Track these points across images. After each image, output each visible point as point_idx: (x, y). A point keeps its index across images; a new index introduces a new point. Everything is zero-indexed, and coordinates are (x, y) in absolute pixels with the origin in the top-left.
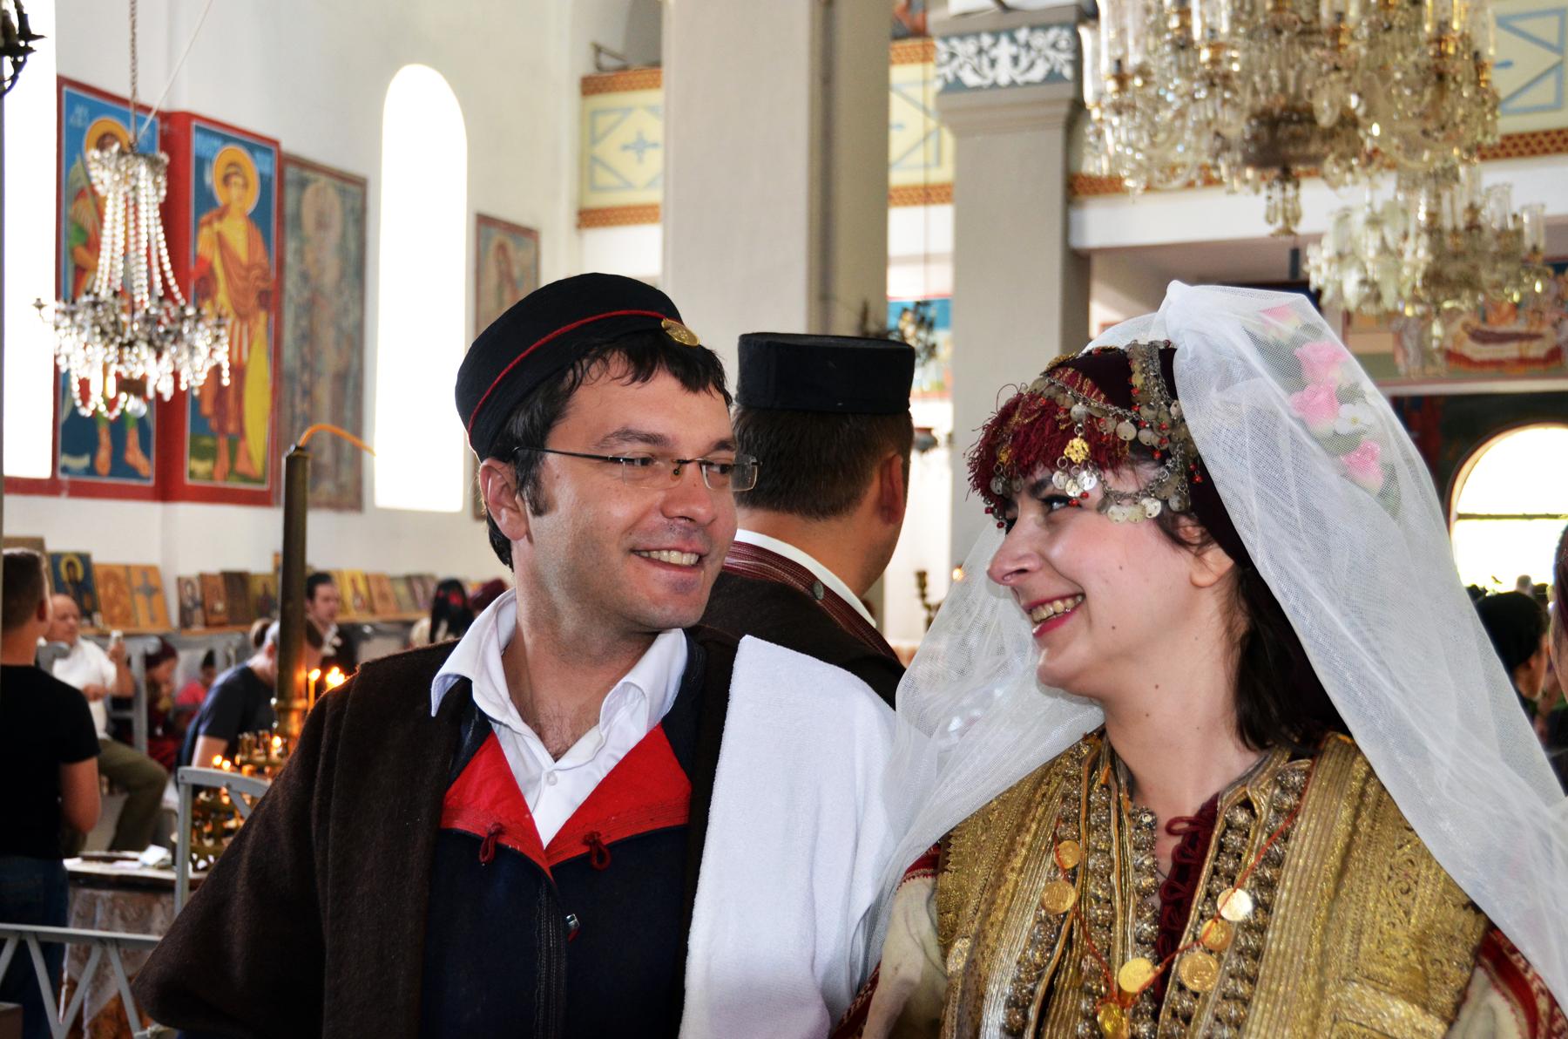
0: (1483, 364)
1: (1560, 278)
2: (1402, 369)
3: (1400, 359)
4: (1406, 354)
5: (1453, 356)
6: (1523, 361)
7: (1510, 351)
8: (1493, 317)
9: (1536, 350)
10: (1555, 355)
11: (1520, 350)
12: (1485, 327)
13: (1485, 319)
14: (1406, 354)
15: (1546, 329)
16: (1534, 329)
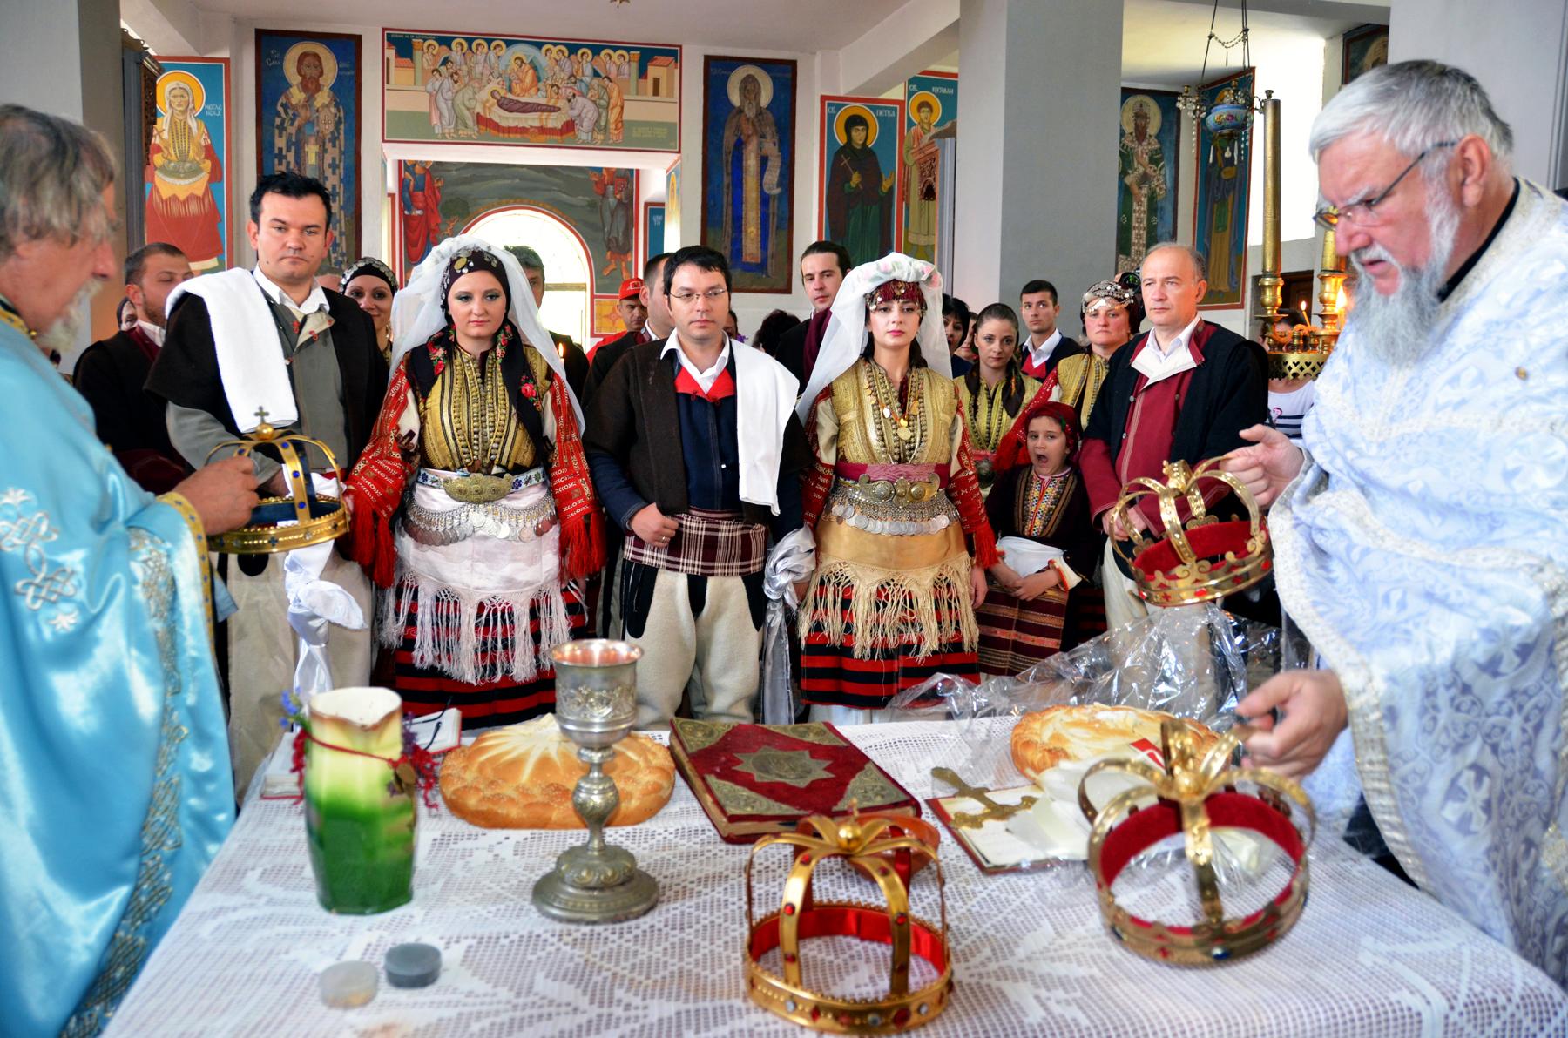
0: (509, 130)
1: (573, 57)
2: (437, 130)
3: (435, 120)
4: (441, 116)
5: (480, 120)
6: (543, 130)
7: (532, 120)
8: (517, 89)
9: (555, 121)
10: (569, 127)
11: (541, 119)
12: (510, 96)
13: (510, 90)
14: (441, 116)
15: (561, 103)
16: (551, 104)
